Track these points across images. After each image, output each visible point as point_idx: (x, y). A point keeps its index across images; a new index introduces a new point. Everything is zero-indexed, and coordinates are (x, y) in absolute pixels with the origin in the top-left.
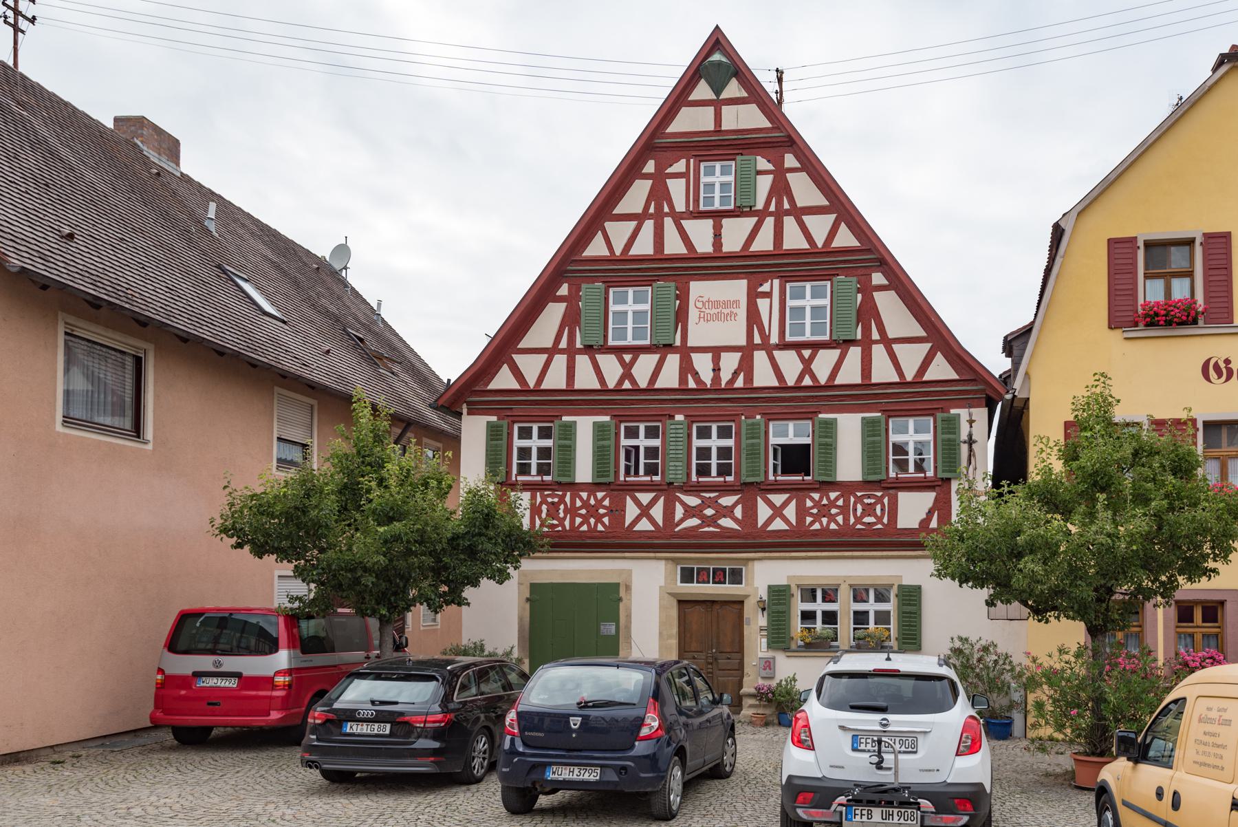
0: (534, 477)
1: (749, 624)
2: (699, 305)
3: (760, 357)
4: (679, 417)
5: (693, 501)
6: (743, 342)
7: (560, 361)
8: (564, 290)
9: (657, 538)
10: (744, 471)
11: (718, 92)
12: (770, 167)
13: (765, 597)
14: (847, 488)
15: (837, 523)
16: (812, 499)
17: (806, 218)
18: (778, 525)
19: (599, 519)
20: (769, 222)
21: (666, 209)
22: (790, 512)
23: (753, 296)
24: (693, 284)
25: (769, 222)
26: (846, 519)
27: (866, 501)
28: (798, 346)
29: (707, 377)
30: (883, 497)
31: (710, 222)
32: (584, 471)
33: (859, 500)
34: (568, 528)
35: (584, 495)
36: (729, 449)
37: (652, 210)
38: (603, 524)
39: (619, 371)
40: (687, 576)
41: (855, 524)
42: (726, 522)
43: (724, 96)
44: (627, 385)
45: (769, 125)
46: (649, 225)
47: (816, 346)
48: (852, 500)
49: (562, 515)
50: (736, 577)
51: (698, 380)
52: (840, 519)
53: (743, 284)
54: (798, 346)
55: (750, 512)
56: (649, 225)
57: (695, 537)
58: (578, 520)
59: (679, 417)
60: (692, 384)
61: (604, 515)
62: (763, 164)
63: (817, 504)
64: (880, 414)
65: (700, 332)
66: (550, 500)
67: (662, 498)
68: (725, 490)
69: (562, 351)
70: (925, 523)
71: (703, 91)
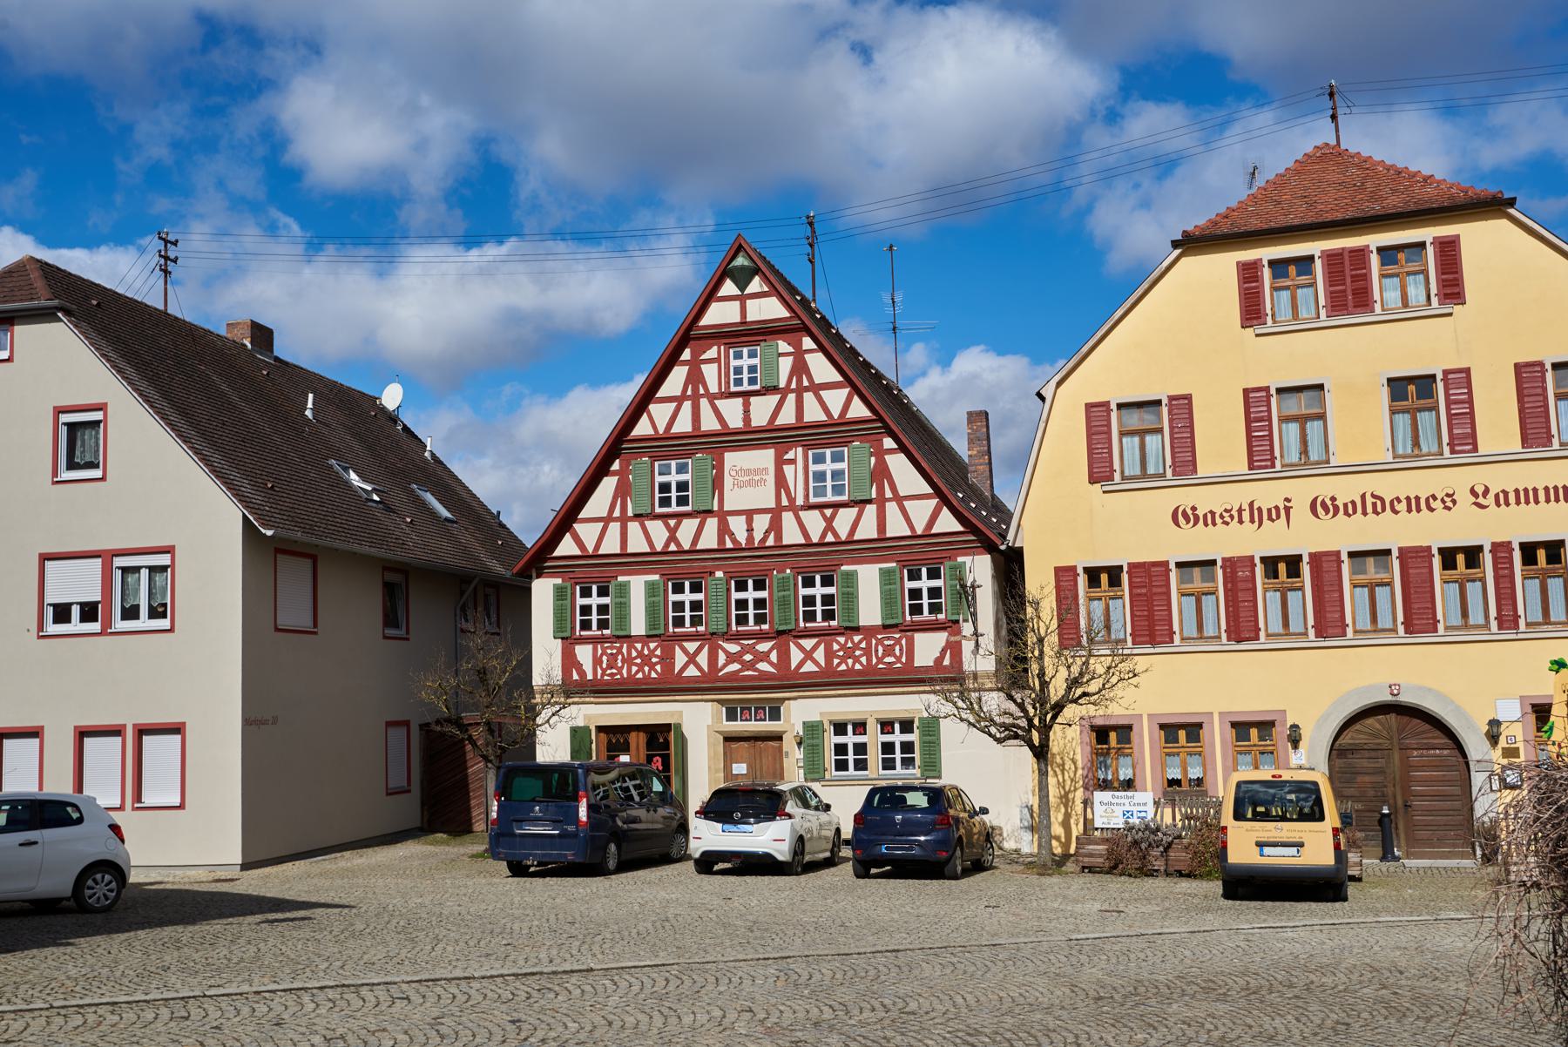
0: (594, 631)
1: (787, 756)
2: (733, 473)
3: (788, 518)
4: (719, 574)
5: (733, 648)
6: (772, 505)
7: (615, 527)
8: (616, 466)
9: (703, 683)
10: (776, 620)
11: (742, 289)
12: (791, 349)
13: (801, 733)
14: (869, 632)
15: (861, 664)
16: (838, 643)
17: (823, 393)
18: (809, 667)
19: (652, 667)
20: (791, 397)
21: (702, 391)
22: (820, 655)
23: (780, 463)
24: (727, 455)
25: (791, 397)
26: (869, 660)
27: (887, 643)
28: (820, 507)
29: (742, 537)
30: (901, 638)
31: (740, 400)
32: (638, 626)
33: (880, 642)
34: (625, 675)
35: (639, 646)
36: (607, 606)
37: (689, 393)
38: (656, 671)
40: (731, 716)
41: (877, 663)
42: (763, 666)
43: (749, 290)
44: (673, 547)
45: (788, 315)
46: (687, 405)
47: (836, 506)
48: (874, 642)
49: (620, 665)
50: (775, 715)
51: (734, 541)
52: (864, 660)
53: (770, 454)
54: (820, 507)
55: (785, 656)
56: (687, 405)
57: (736, 680)
58: (634, 669)
59: (719, 574)
60: (729, 545)
61: (657, 663)
62: (783, 346)
63: (843, 647)
64: (894, 564)
65: (734, 498)
66: (609, 651)
67: (707, 646)
68: (761, 637)
69: (616, 520)
70: (939, 660)
71: (729, 288)
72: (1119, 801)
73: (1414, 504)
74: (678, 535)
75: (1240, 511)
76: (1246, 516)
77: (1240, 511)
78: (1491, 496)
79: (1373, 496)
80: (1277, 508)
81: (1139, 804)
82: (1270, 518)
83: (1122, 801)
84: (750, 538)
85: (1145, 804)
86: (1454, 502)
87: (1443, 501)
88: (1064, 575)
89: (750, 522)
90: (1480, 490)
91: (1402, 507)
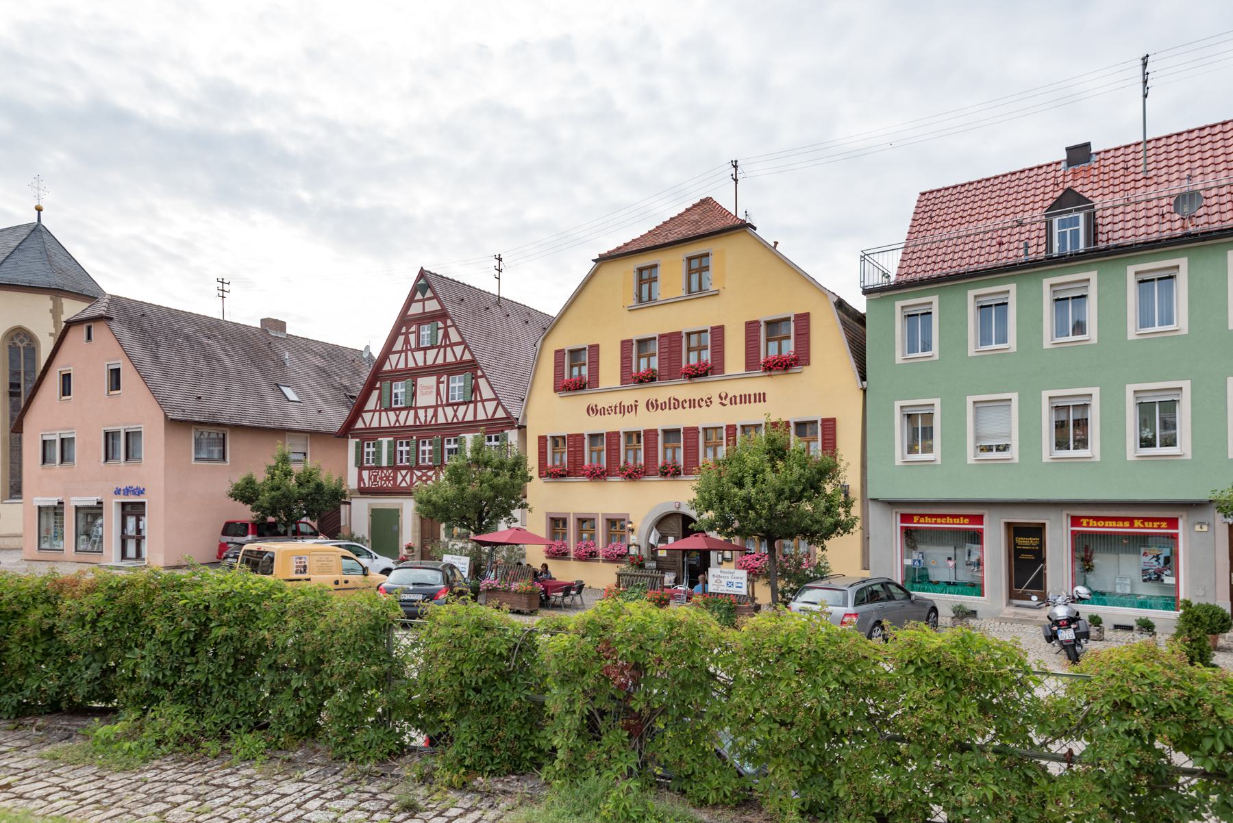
5: (419, 474)
20: (442, 350)
23: (439, 383)
24: (419, 379)
25: (442, 350)
28: (452, 405)
32: (384, 463)
35: (385, 471)
39: (395, 418)
46: (403, 354)
47: (458, 404)
51: (420, 422)
53: (435, 378)
54: (452, 405)
60: (418, 423)
65: (422, 400)
71: (419, 296)
72: (725, 575)
73: (693, 404)
74: (458, 413)
75: (616, 407)
76: (618, 409)
77: (616, 407)
78: (728, 399)
79: (674, 399)
80: (631, 405)
81: (737, 578)
82: (628, 412)
83: (727, 575)
84: (426, 420)
85: (741, 578)
86: (711, 402)
87: (706, 402)
88: (542, 440)
89: (426, 412)
90: (723, 396)
91: (687, 405)
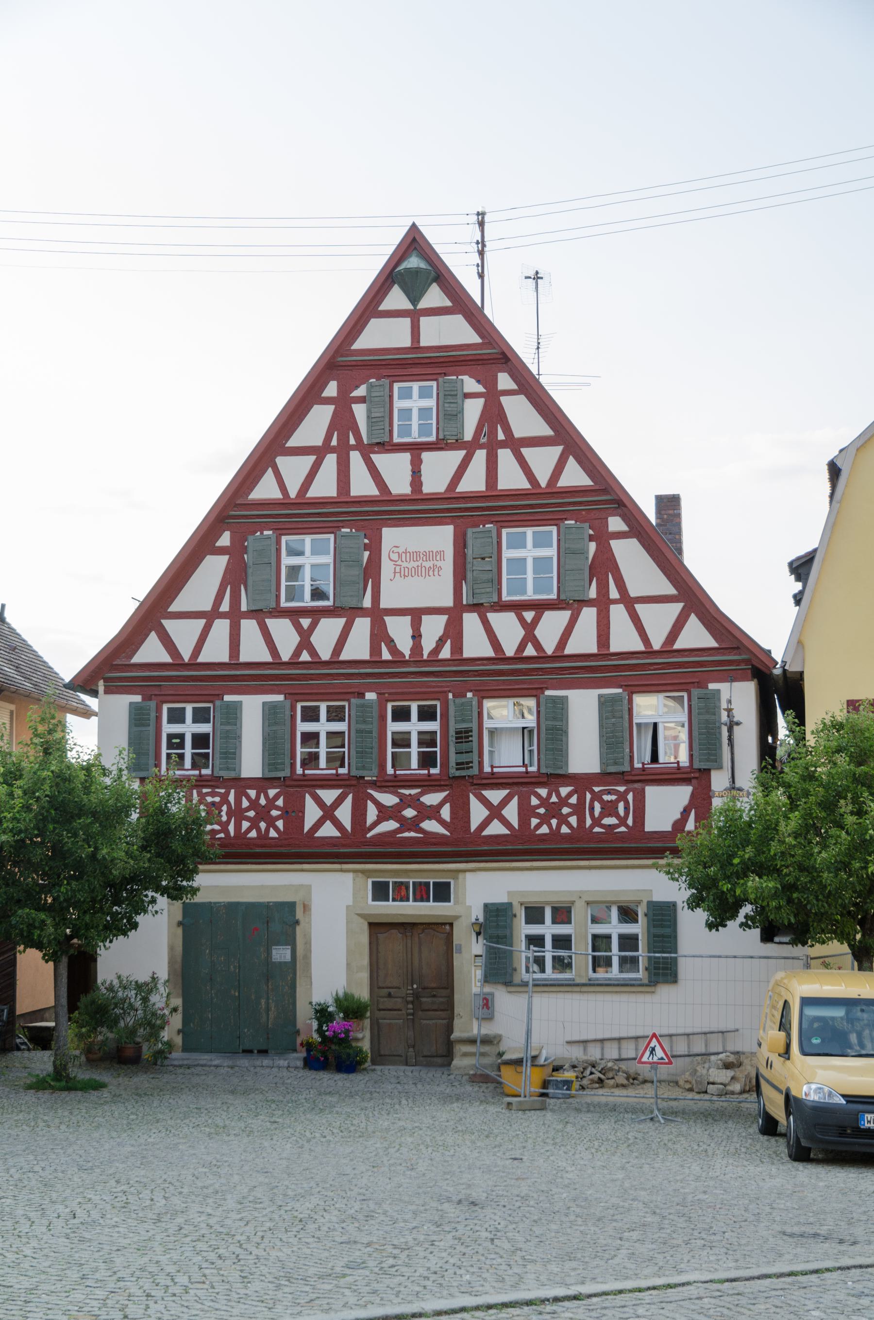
0: (188, 769)
1: (460, 951)
2: (395, 557)
3: (471, 622)
4: (371, 696)
5: (388, 799)
6: (449, 602)
7: (222, 627)
8: (225, 540)
9: (344, 846)
11: (414, 300)
12: (480, 389)
13: (481, 920)
14: (582, 782)
15: (569, 825)
16: (538, 796)
17: (525, 451)
18: (496, 828)
19: (271, 823)
20: (480, 456)
21: (352, 441)
22: (511, 812)
25: (480, 456)
26: (581, 821)
27: (606, 798)
29: (405, 645)
30: (626, 792)
31: (406, 457)
33: (596, 797)
34: (232, 834)
35: (252, 793)
37: (334, 442)
38: (276, 829)
39: (295, 639)
40: (380, 891)
41: (592, 826)
42: (431, 826)
43: (423, 304)
44: (305, 657)
45: (478, 340)
47: (540, 607)
48: (588, 796)
49: (224, 818)
50: (442, 892)
51: (393, 649)
52: (573, 820)
53: (448, 531)
55: (461, 812)
56: (331, 461)
57: (391, 844)
58: (245, 825)
59: (371, 696)
60: (386, 655)
61: (278, 818)
62: (470, 384)
63: (544, 802)
64: (620, 690)
66: (209, 799)
67: (350, 796)
68: (429, 784)
69: (223, 616)
70: (679, 825)
71: (396, 299)
84: (417, 647)
